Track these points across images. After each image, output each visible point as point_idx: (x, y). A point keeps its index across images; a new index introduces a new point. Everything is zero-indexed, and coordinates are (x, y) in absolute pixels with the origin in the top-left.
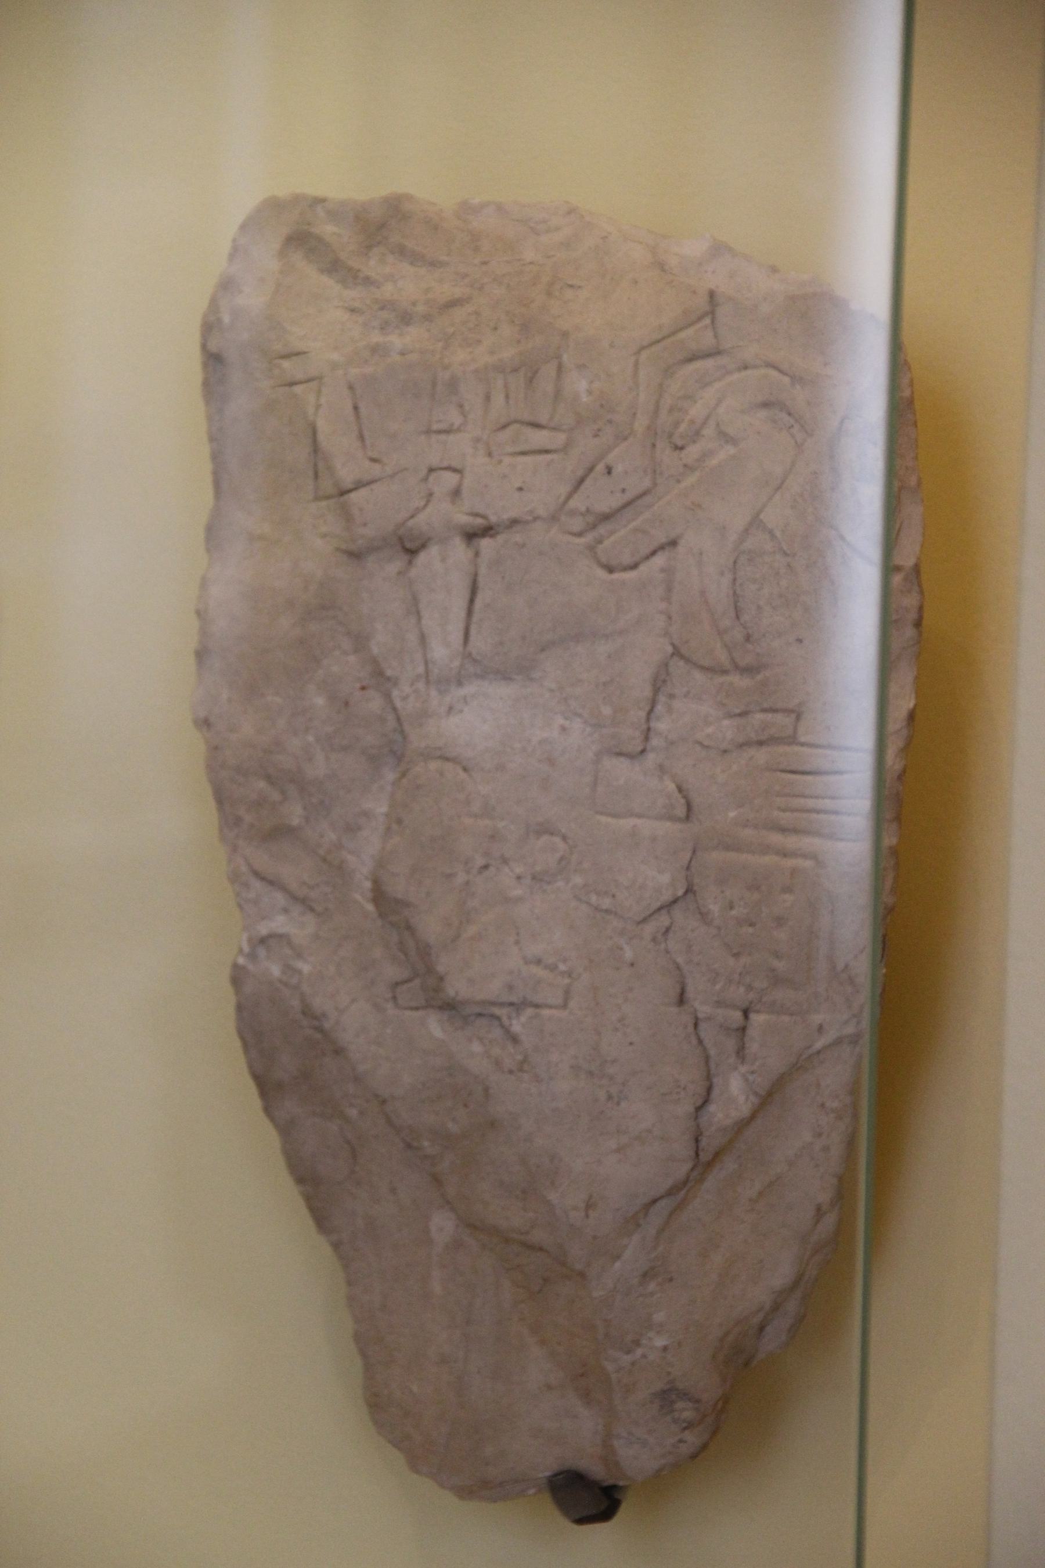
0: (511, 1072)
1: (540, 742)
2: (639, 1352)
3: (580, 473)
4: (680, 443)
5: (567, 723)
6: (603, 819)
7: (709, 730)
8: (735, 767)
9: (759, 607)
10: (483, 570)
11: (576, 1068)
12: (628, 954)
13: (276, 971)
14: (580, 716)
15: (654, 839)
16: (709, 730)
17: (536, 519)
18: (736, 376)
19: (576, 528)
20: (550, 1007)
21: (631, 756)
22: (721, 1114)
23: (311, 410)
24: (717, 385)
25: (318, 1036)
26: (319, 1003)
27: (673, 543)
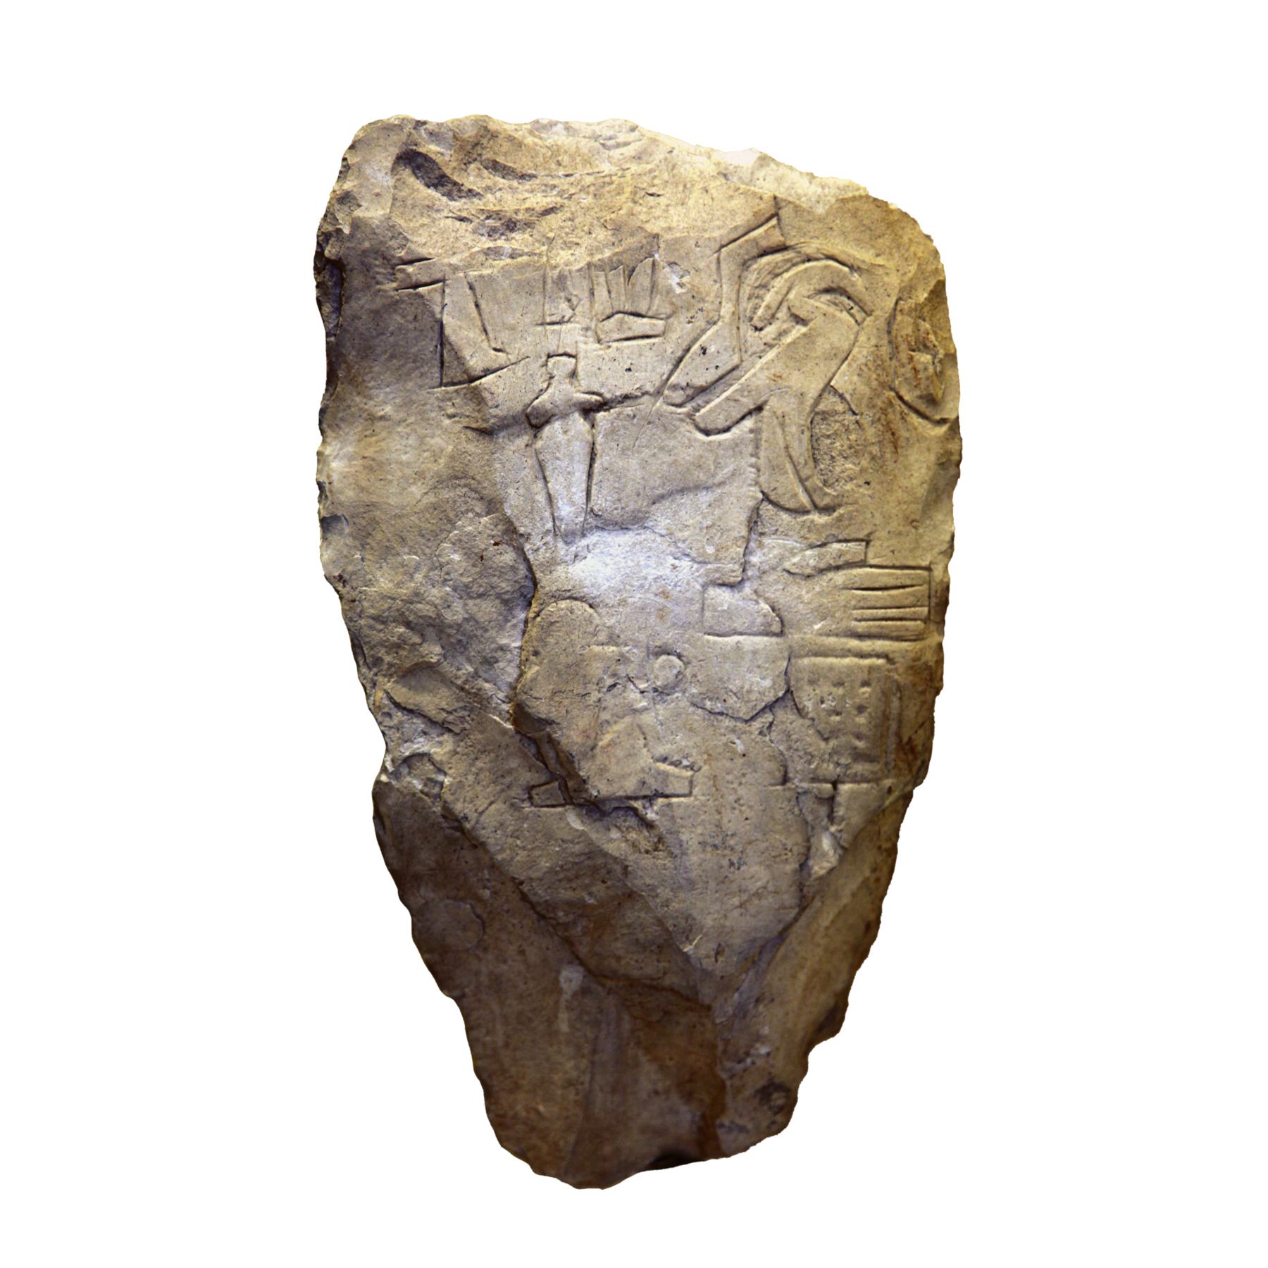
0: (647, 852)
1: (656, 579)
2: (749, 1061)
3: (679, 354)
4: (759, 326)
5: (676, 562)
6: (711, 638)
7: (796, 560)
8: (818, 589)
9: (833, 457)
10: (599, 439)
11: (703, 844)
12: (740, 747)
13: (418, 785)
14: (688, 555)
15: (755, 652)
16: (796, 560)
17: (646, 393)
18: (802, 267)
19: (678, 401)
20: (678, 796)
21: (731, 586)
22: (819, 868)
23: (437, 309)
24: (786, 275)
25: (458, 834)
26: (458, 807)
27: (759, 409)
